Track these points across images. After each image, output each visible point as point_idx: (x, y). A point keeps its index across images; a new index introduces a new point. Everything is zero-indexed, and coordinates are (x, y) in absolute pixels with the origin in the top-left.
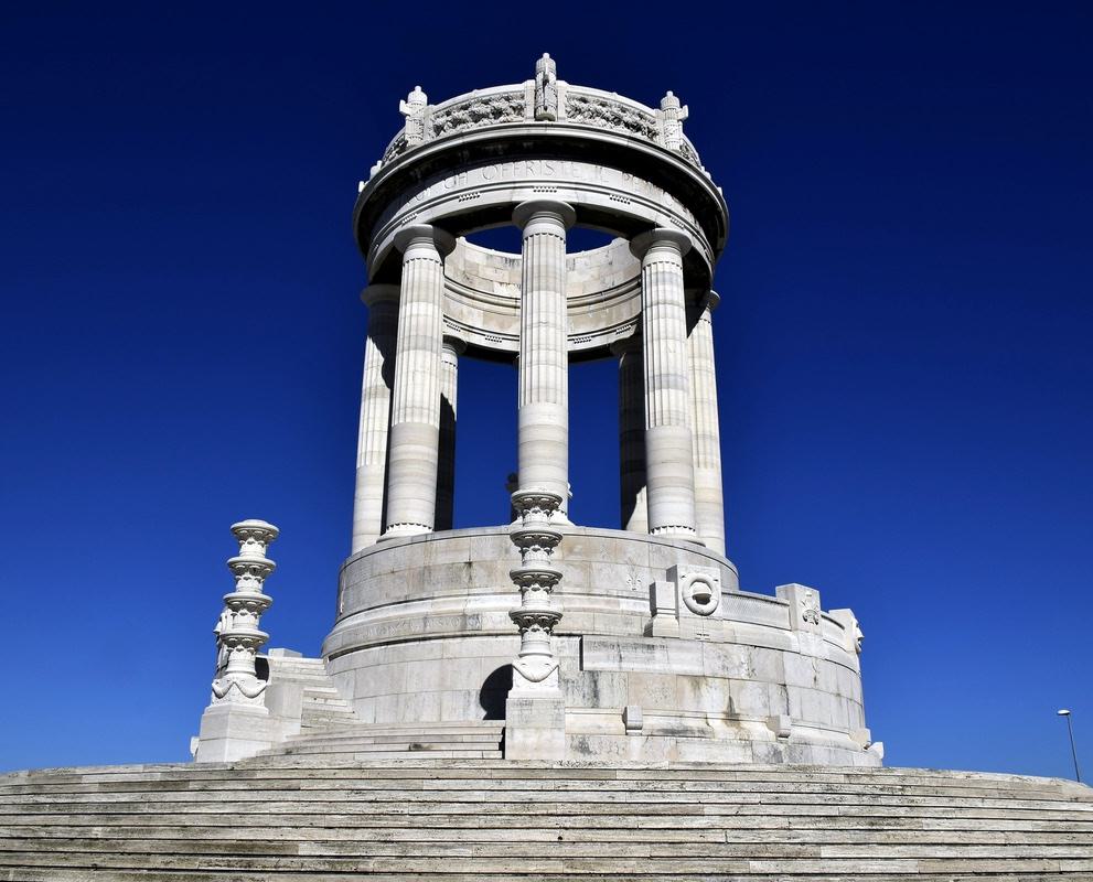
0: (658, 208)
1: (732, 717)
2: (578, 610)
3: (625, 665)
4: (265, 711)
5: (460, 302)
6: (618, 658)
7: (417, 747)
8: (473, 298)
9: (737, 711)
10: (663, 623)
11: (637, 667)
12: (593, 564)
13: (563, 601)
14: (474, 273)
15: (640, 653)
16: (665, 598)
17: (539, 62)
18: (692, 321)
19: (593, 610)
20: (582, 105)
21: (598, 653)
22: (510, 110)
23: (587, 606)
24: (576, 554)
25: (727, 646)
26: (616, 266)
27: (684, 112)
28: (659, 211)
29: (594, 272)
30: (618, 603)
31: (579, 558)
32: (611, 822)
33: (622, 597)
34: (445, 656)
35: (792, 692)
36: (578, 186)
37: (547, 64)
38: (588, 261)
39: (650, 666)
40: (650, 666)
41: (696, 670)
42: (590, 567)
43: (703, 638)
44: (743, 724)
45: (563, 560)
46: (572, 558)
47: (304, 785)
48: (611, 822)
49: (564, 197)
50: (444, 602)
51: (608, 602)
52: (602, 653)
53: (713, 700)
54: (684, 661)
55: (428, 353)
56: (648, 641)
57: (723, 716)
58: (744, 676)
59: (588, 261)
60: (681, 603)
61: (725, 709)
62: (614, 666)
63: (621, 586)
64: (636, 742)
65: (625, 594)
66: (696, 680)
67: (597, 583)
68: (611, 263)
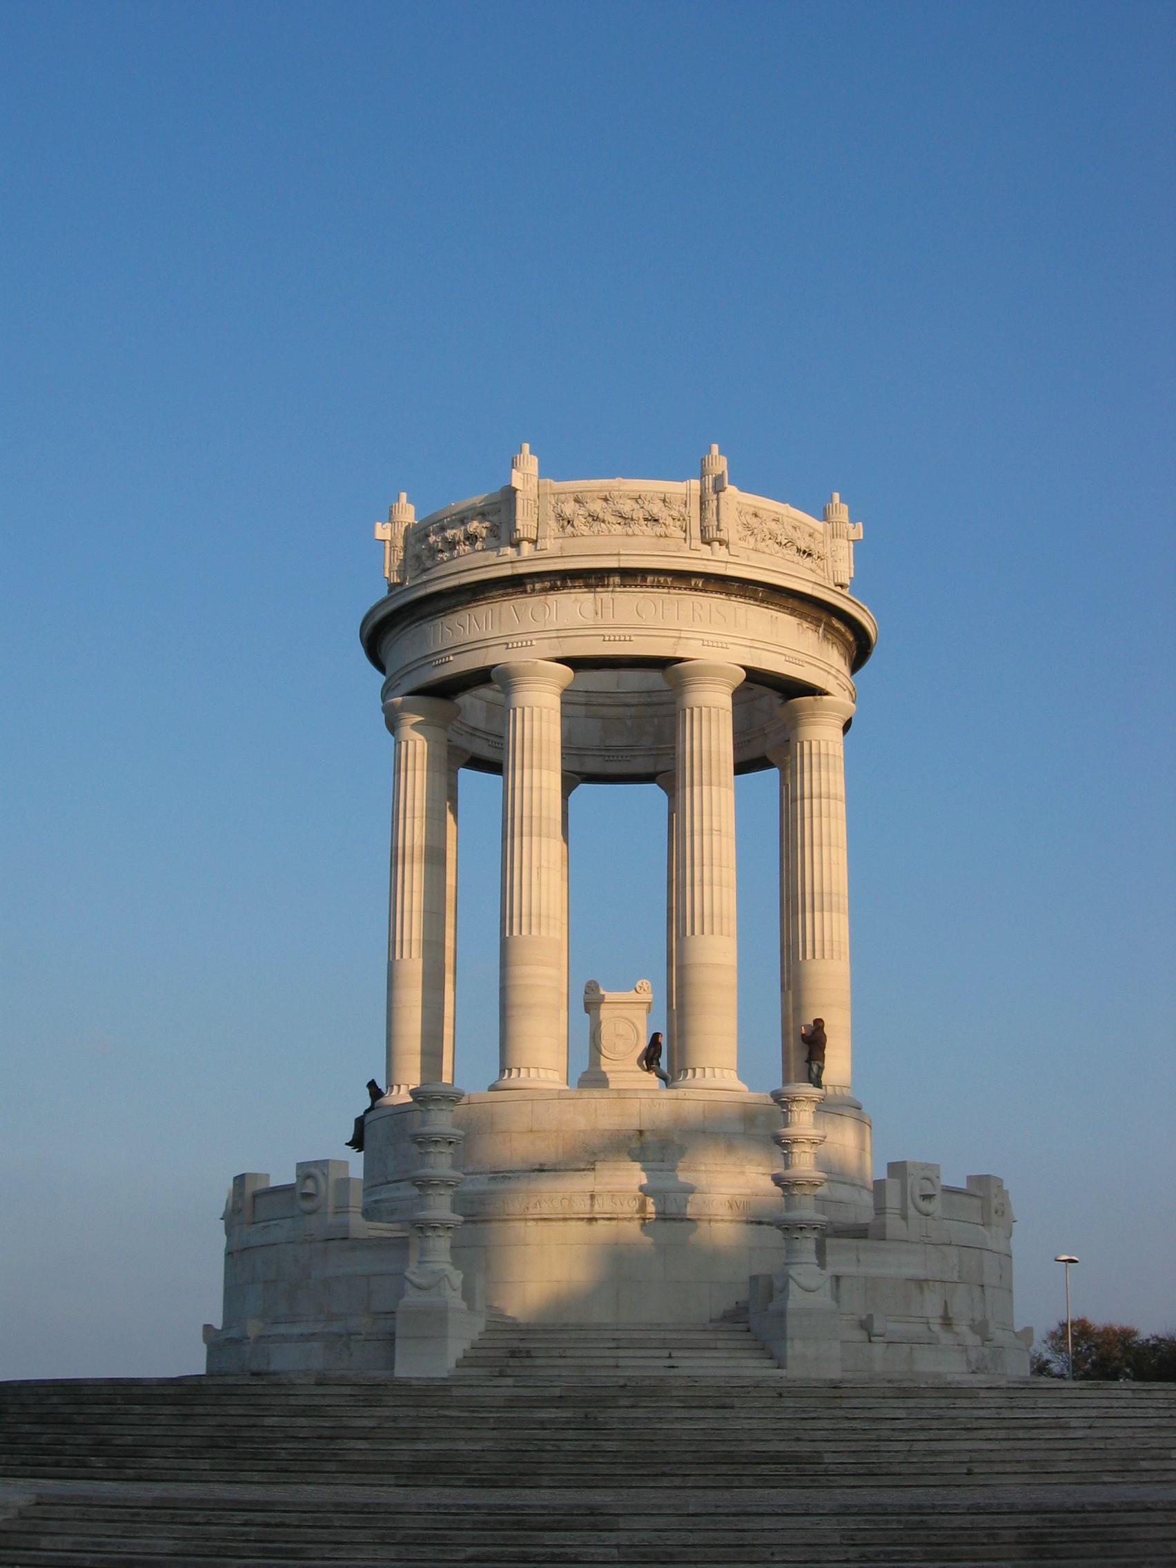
4: (464, 1305)
9: (951, 1315)
10: (893, 1224)
16: (893, 1199)
20: (754, 522)
22: (669, 521)
25: (944, 1248)
27: (857, 531)
32: (1021, 1434)
35: (988, 1291)
37: (719, 463)
41: (921, 1273)
43: (926, 1240)
44: (956, 1329)
47: (737, 1403)
48: (1021, 1434)
53: (932, 1306)
57: (940, 1321)
58: (956, 1279)
61: (940, 1312)
64: (878, 1349)
66: (921, 1283)
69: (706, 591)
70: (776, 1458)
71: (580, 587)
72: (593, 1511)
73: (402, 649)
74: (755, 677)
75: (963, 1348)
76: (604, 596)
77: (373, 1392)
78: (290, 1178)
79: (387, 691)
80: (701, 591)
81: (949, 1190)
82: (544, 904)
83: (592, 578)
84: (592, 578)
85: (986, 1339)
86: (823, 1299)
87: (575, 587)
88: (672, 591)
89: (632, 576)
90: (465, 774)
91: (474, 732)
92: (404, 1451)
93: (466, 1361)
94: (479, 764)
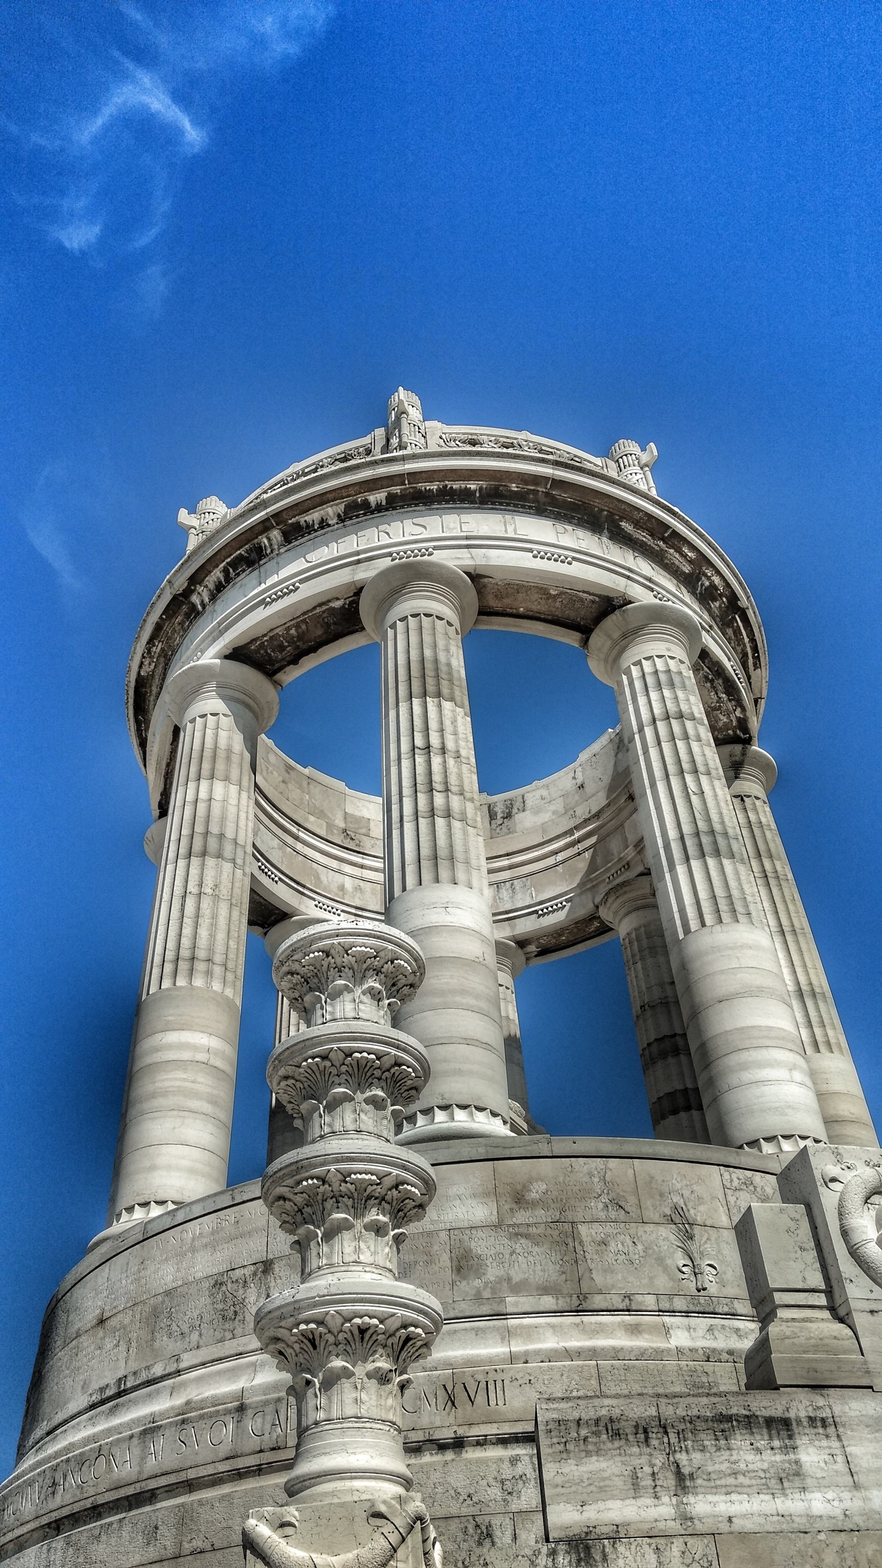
0: (629, 575)
2: (551, 1356)
3: (705, 1505)
5: (339, 872)
6: (670, 1481)
8: (362, 867)
11: (748, 1508)
12: (583, 1229)
13: (508, 1335)
14: (364, 831)
15: (750, 1454)
17: (395, 399)
18: (734, 770)
19: (593, 1353)
21: (595, 1464)
23: (575, 1343)
24: (534, 1204)
26: (590, 788)
28: (628, 578)
29: (558, 805)
30: (666, 1331)
31: (541, 1214)
33: (672, 1312)
34: (187, 1547)
36: (470, 542)
38: (545, 793)
39: (792, 1504)
40: (792, 1504)
42: (574, 1235)
45: (498, 1226)
46: (521, 1217)
49: (454, 560)
50: (199, 1379)
51: (635, 1330)
52: (608, 1465)
55: (227, 867)
56: (765, 1404)
59: (545, 793)
60: (846, 1266)
62: (659, 1510)
63: (663, 1283)
65: (680, 1304)
67: (598, 1278)
68: (582, 786)
69: (394, 509)
71: (244, 571)
80: (387, 510)
82: (186, 942)
87: (238, 575)
88: (348, 523)
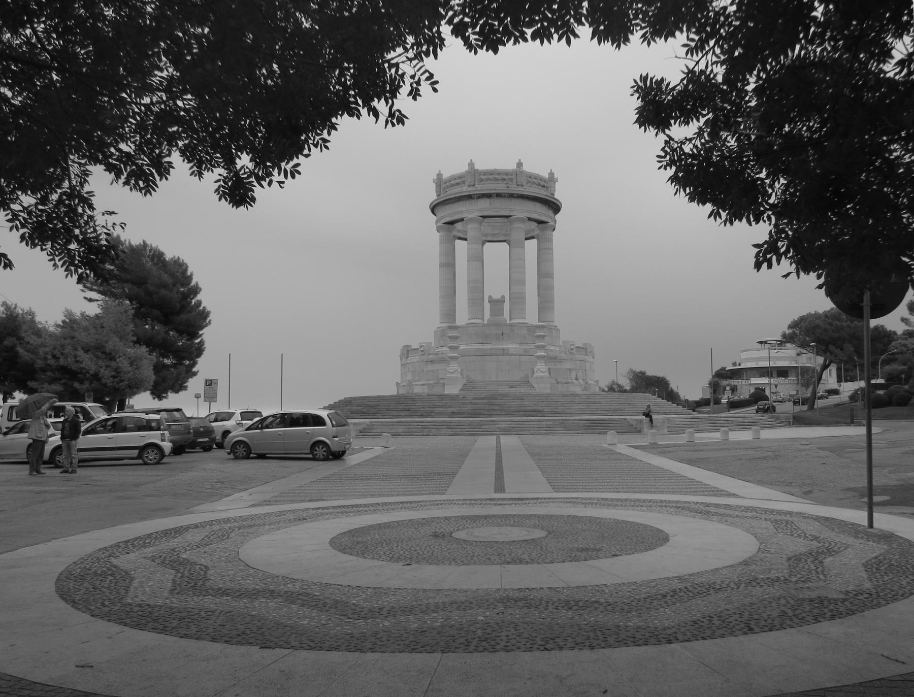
1: (577, 379)
7: (511, 387)
53: (573, 375)
54: (568, 365)
64: (560, 386)
66: (570, 370)
70: (534, 410)
72: (492, 421)
73: (442, 212)
74: (530, 219)
75: (580, 385)
76: (492, 200)
77: (442, 397)
78: (417, 346)
79: (437, 222)
81: (577, 347)
83: (489, 196)
84: (489, 196)
85: (587, 383)
86: (547, 374)
89: (499, 195)
90: (458, 242)
91: (459, 231)
92: (450, 410)
93: (461, 390)
94: (460, 238)
